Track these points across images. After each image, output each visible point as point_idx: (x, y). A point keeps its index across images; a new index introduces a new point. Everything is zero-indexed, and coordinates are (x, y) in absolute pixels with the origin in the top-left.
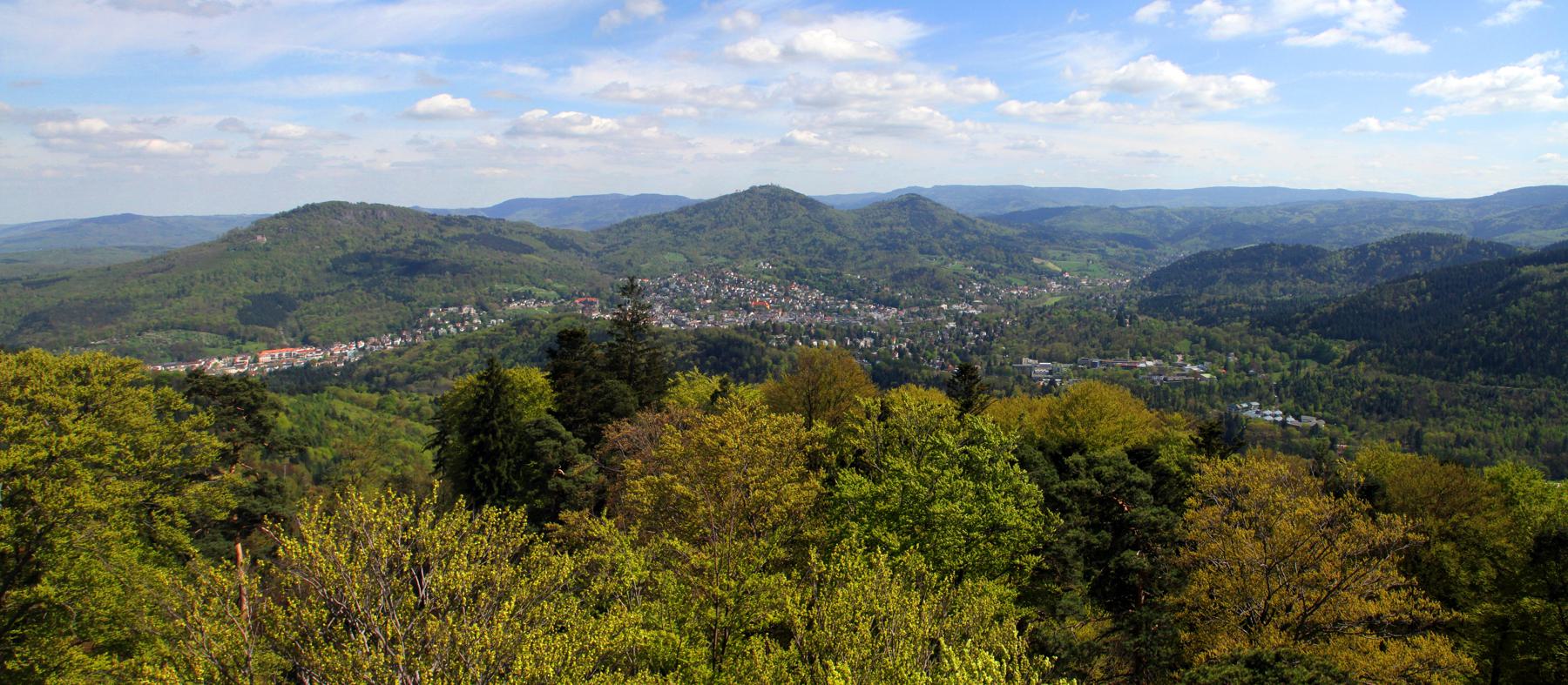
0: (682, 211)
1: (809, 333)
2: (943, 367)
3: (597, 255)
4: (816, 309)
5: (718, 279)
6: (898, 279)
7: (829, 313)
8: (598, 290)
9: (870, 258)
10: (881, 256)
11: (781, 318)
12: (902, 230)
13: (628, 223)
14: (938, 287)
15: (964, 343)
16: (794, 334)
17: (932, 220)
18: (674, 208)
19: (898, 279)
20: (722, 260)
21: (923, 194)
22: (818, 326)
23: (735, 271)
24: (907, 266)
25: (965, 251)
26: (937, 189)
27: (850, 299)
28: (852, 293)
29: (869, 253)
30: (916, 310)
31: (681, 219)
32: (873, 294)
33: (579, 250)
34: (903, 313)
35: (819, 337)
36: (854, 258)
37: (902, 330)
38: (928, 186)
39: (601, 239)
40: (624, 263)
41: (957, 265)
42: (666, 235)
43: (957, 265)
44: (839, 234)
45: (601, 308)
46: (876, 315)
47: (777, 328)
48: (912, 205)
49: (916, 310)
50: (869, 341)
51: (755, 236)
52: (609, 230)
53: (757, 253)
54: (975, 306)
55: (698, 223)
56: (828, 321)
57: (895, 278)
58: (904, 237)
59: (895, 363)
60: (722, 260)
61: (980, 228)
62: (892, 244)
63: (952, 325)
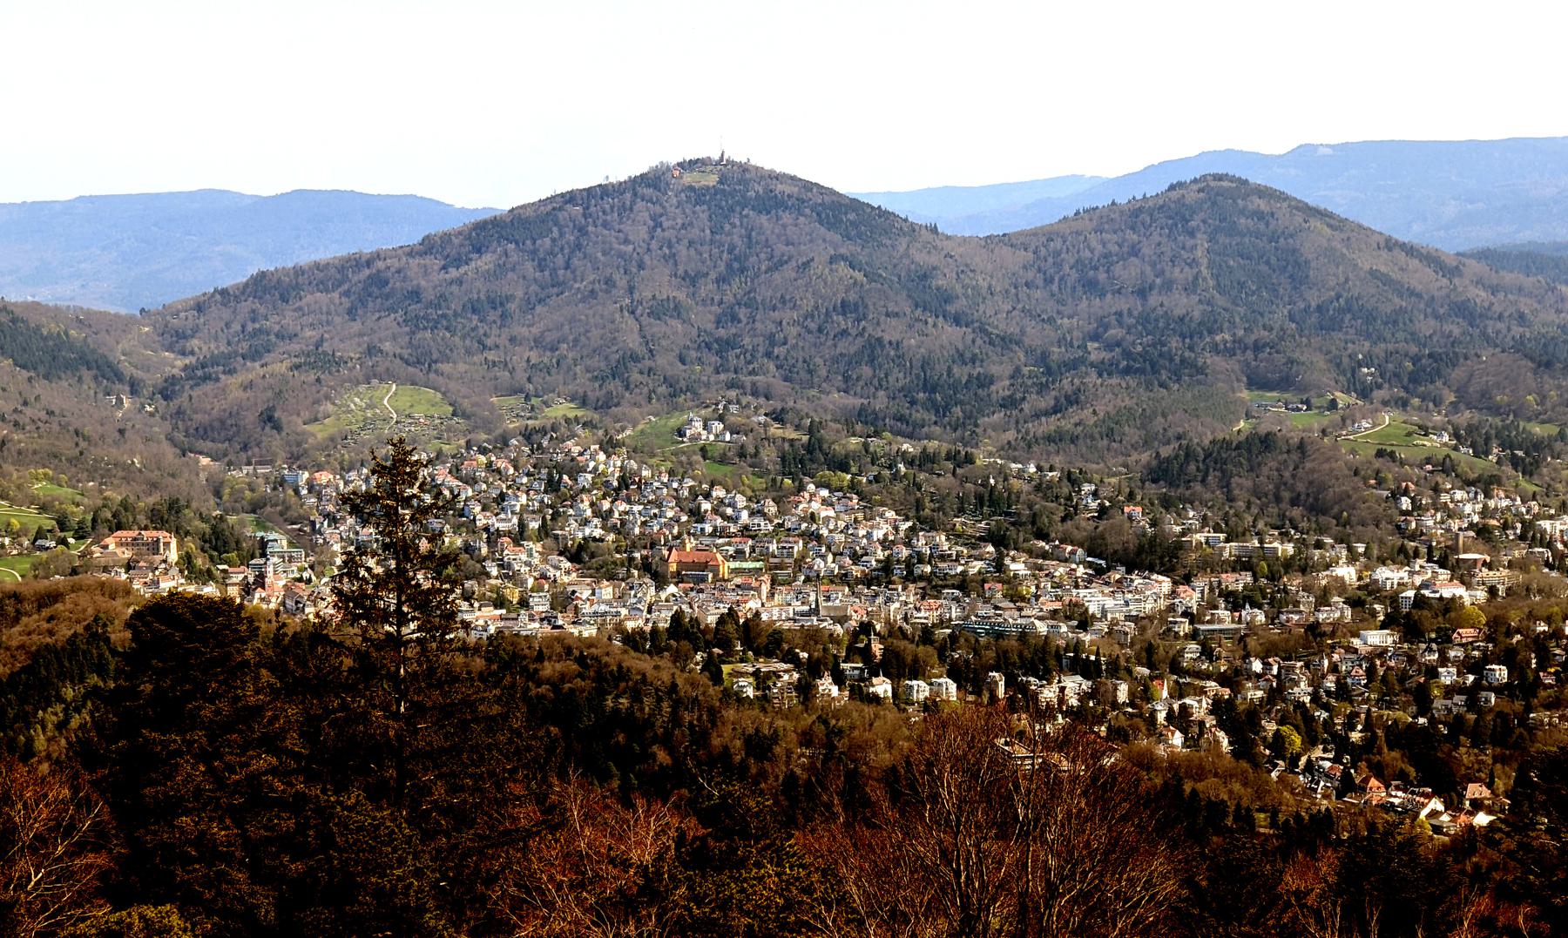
0: (429, 246)
1: (866, 654)
2: (1347, 786)
3: (167, 391)
4: (882, 576)
5: (558, 483)
6: (1171, 477)
7: (932, 587)
8: (174, 506)
9: (1073, 400)
10: (1110, 397)
11: (775, 608)
12: (1180, 303)
13: (261, 285)
14: (1319, 507)
15: (1422, 700)
16: (814, 655)
17: (1295, 269)
18: (413, 237)
19: (1171, 477)
20: (562, 409)
21: (1257, 178)
22: (894, 632)
23: (609, 446)
24: (1204, 433)
25: (1416, 378)
26: (1304, 154)
27: (1000, 540)
28: (1010, 522)
29: (1067, 384)
30: (1238, 582)
31: (430, 277)
32: (1084, 523)
33: (107, 373)
34: (1191, 598)
35: (899, 667)
36: (1009, 403)
37: (1192, 650)
38: (1275, 142)
39: (175, 338)
40: (250, 418)
41: (1377, 425)
42: (389, 331)
43: (1377, 425)
44: (957, 321)
45: (187, 561)
46: (1095, 599)
47: (762, 640)
48: (1215, 213)
49: (1238, 582)
50: (1074, 685)
51: (674, 332)
52: (199, 307)
53: (676, 393)
54: (1462, 572)
55: (480, 289)
56: (927, 614)
57: (1160, 473)
58: (1191, 331)
59: (1173, 764)
60: (562, 409)
61: (1480, 296)
62: (1154, 359)
63: (1377, 638)
